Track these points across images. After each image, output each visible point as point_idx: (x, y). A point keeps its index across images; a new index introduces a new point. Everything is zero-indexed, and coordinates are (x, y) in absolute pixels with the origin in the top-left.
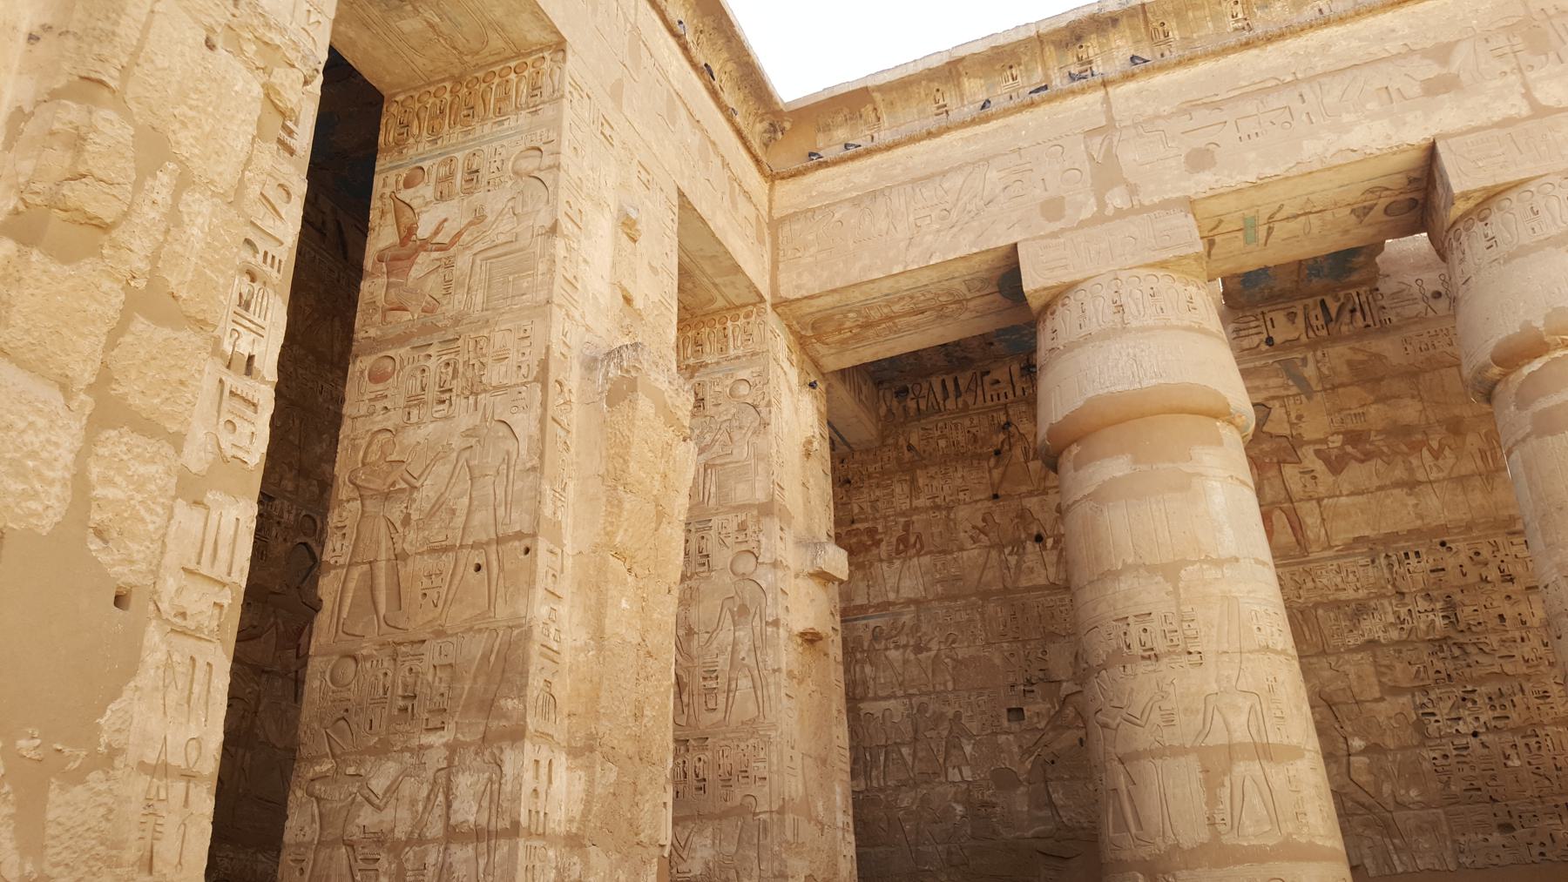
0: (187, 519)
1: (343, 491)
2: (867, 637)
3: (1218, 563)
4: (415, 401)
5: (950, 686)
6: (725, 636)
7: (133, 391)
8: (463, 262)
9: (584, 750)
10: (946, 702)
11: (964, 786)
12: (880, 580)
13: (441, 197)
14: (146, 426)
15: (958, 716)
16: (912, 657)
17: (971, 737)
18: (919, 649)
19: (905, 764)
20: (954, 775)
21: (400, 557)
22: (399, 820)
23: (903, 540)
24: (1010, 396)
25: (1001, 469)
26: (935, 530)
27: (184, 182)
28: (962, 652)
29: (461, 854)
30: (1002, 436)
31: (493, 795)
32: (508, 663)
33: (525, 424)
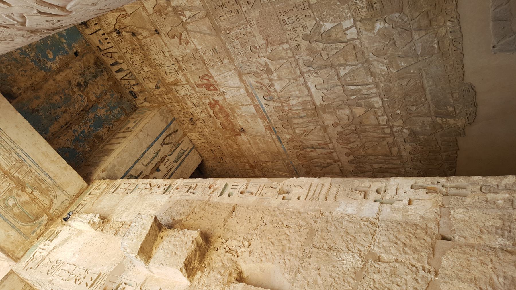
5: (286, 46)
10: (298, 47)
11: (359, 24)
12: (236, 99)
15: (305, 37)
16: (275, 74)
17: (318, 25)
18: (268, 71)
19: (352, 71)
20: (352, 33)
23: (208, 86)
24: (102, 32)
25: (141, 31)
26: (193, 68)
28: (260, 41)
30: (124, 33)
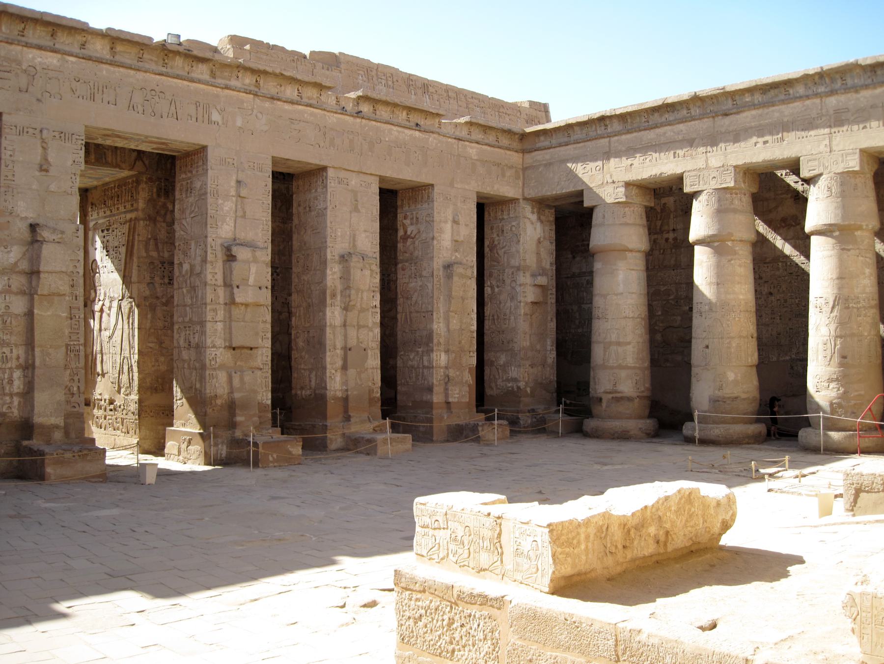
0: (371, 334)
1: (399, 296)
2: (585, 283)
3: (616, 295)
4: (410, 277)
6: (508, 304)
7: (361, 323)
8: (417, 242)
9: (447, 351)
13: (412, 224)
14: (364, 327)
21: (411, 312)
22: (415, 363)
27: (362, 292)
29: (425, 371)
31: (430, 361)
32: (430, 337)
33: (430, 285)
